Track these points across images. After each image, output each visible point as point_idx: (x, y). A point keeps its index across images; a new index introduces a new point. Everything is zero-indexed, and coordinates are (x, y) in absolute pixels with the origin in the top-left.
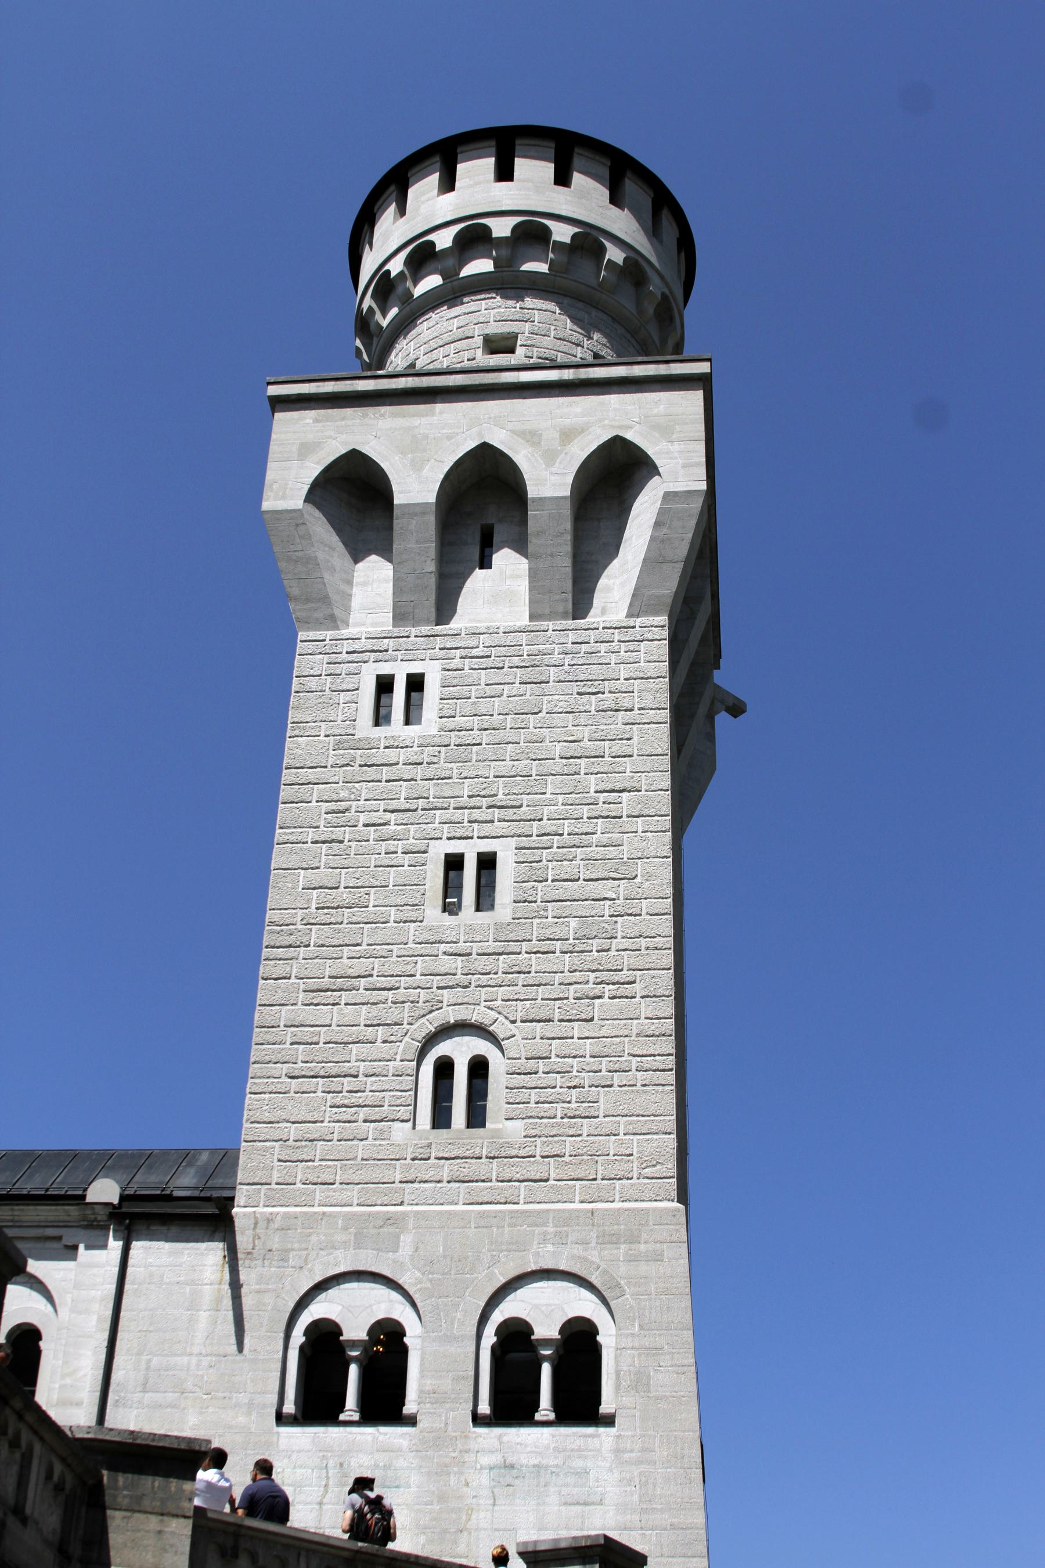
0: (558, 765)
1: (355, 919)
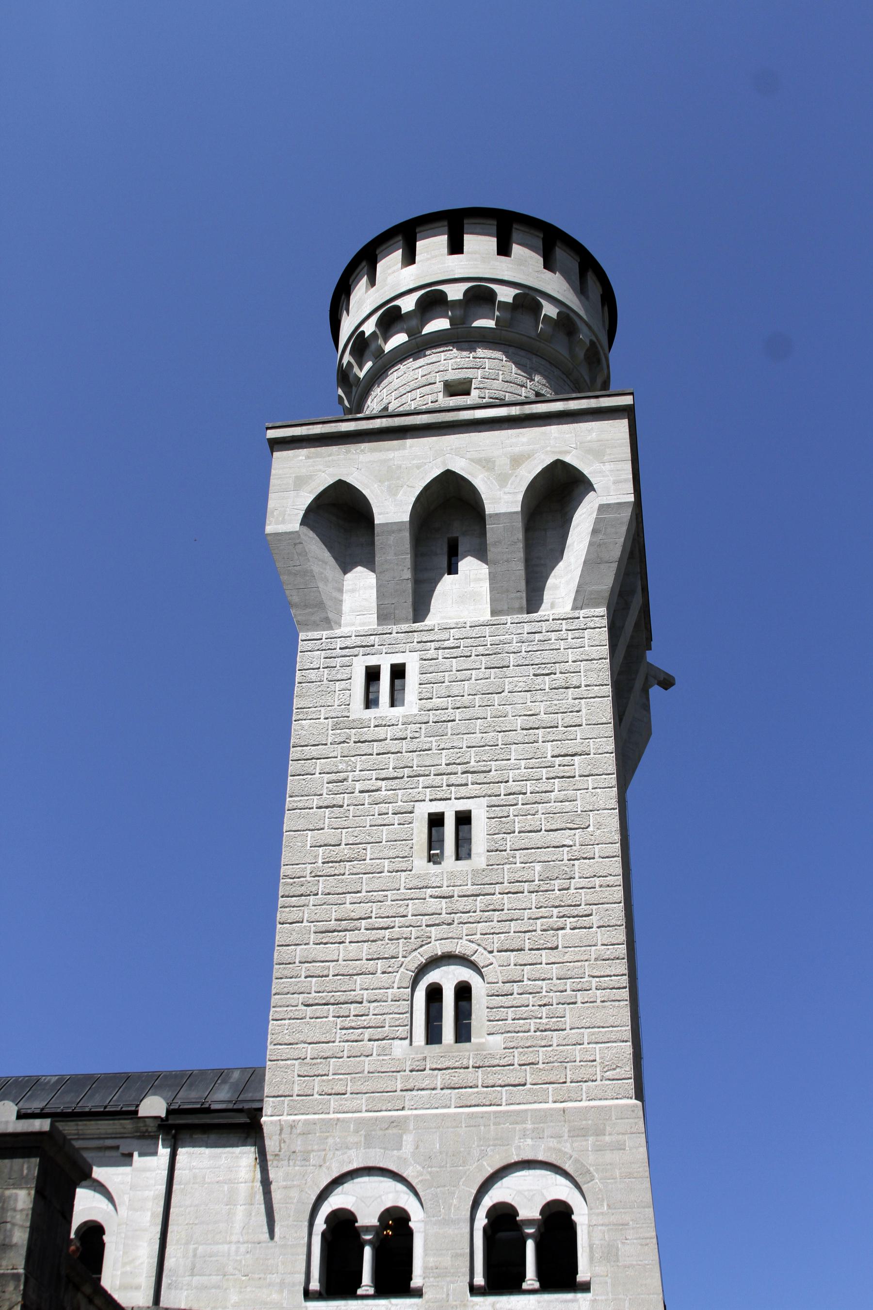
0: (520, 735)
1: (355, 871)
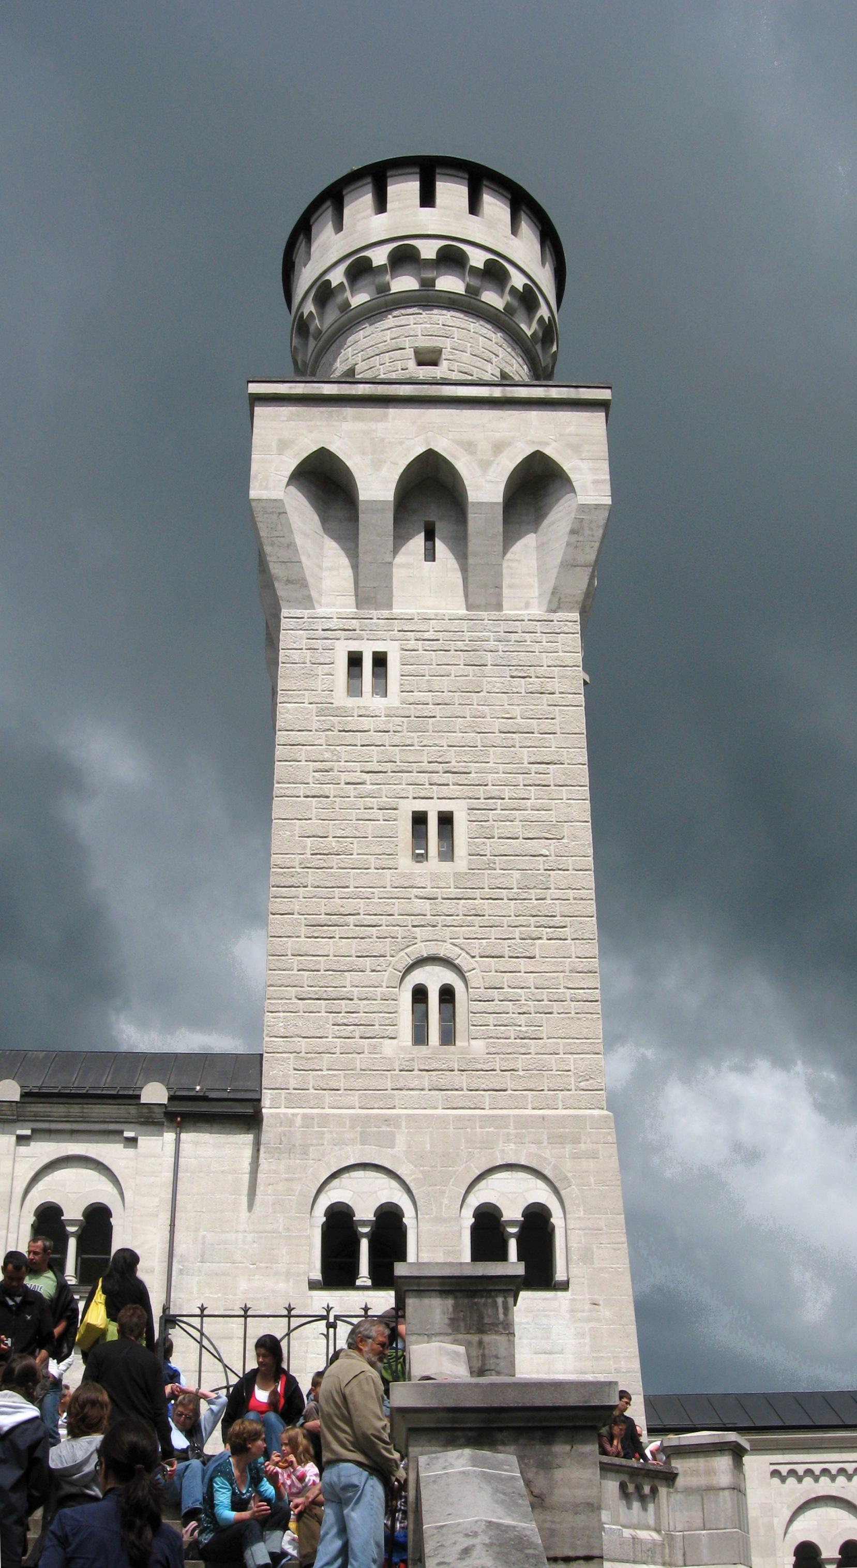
0: (498, 738)
1: (342, 865)
